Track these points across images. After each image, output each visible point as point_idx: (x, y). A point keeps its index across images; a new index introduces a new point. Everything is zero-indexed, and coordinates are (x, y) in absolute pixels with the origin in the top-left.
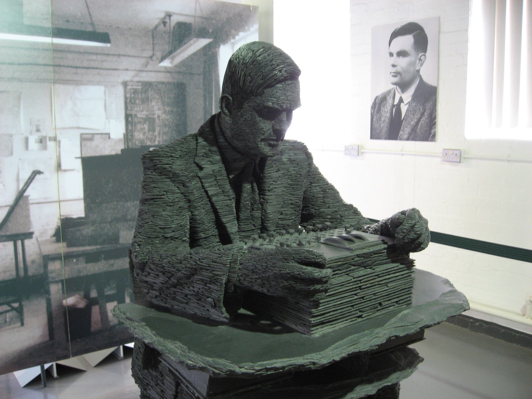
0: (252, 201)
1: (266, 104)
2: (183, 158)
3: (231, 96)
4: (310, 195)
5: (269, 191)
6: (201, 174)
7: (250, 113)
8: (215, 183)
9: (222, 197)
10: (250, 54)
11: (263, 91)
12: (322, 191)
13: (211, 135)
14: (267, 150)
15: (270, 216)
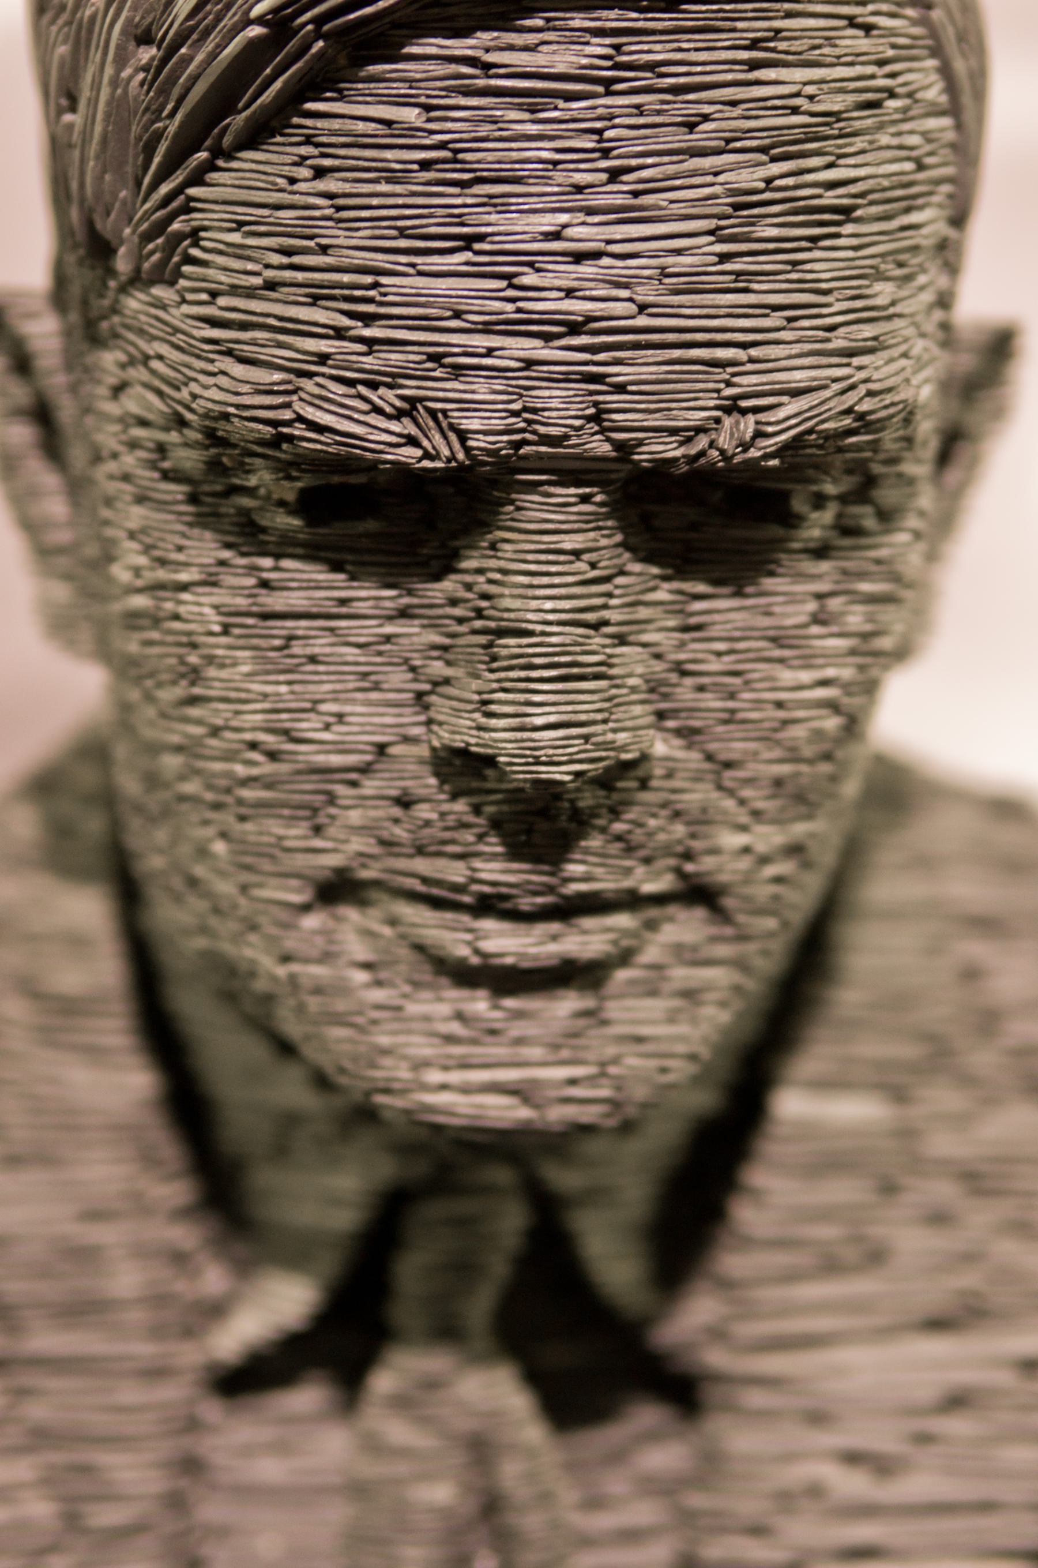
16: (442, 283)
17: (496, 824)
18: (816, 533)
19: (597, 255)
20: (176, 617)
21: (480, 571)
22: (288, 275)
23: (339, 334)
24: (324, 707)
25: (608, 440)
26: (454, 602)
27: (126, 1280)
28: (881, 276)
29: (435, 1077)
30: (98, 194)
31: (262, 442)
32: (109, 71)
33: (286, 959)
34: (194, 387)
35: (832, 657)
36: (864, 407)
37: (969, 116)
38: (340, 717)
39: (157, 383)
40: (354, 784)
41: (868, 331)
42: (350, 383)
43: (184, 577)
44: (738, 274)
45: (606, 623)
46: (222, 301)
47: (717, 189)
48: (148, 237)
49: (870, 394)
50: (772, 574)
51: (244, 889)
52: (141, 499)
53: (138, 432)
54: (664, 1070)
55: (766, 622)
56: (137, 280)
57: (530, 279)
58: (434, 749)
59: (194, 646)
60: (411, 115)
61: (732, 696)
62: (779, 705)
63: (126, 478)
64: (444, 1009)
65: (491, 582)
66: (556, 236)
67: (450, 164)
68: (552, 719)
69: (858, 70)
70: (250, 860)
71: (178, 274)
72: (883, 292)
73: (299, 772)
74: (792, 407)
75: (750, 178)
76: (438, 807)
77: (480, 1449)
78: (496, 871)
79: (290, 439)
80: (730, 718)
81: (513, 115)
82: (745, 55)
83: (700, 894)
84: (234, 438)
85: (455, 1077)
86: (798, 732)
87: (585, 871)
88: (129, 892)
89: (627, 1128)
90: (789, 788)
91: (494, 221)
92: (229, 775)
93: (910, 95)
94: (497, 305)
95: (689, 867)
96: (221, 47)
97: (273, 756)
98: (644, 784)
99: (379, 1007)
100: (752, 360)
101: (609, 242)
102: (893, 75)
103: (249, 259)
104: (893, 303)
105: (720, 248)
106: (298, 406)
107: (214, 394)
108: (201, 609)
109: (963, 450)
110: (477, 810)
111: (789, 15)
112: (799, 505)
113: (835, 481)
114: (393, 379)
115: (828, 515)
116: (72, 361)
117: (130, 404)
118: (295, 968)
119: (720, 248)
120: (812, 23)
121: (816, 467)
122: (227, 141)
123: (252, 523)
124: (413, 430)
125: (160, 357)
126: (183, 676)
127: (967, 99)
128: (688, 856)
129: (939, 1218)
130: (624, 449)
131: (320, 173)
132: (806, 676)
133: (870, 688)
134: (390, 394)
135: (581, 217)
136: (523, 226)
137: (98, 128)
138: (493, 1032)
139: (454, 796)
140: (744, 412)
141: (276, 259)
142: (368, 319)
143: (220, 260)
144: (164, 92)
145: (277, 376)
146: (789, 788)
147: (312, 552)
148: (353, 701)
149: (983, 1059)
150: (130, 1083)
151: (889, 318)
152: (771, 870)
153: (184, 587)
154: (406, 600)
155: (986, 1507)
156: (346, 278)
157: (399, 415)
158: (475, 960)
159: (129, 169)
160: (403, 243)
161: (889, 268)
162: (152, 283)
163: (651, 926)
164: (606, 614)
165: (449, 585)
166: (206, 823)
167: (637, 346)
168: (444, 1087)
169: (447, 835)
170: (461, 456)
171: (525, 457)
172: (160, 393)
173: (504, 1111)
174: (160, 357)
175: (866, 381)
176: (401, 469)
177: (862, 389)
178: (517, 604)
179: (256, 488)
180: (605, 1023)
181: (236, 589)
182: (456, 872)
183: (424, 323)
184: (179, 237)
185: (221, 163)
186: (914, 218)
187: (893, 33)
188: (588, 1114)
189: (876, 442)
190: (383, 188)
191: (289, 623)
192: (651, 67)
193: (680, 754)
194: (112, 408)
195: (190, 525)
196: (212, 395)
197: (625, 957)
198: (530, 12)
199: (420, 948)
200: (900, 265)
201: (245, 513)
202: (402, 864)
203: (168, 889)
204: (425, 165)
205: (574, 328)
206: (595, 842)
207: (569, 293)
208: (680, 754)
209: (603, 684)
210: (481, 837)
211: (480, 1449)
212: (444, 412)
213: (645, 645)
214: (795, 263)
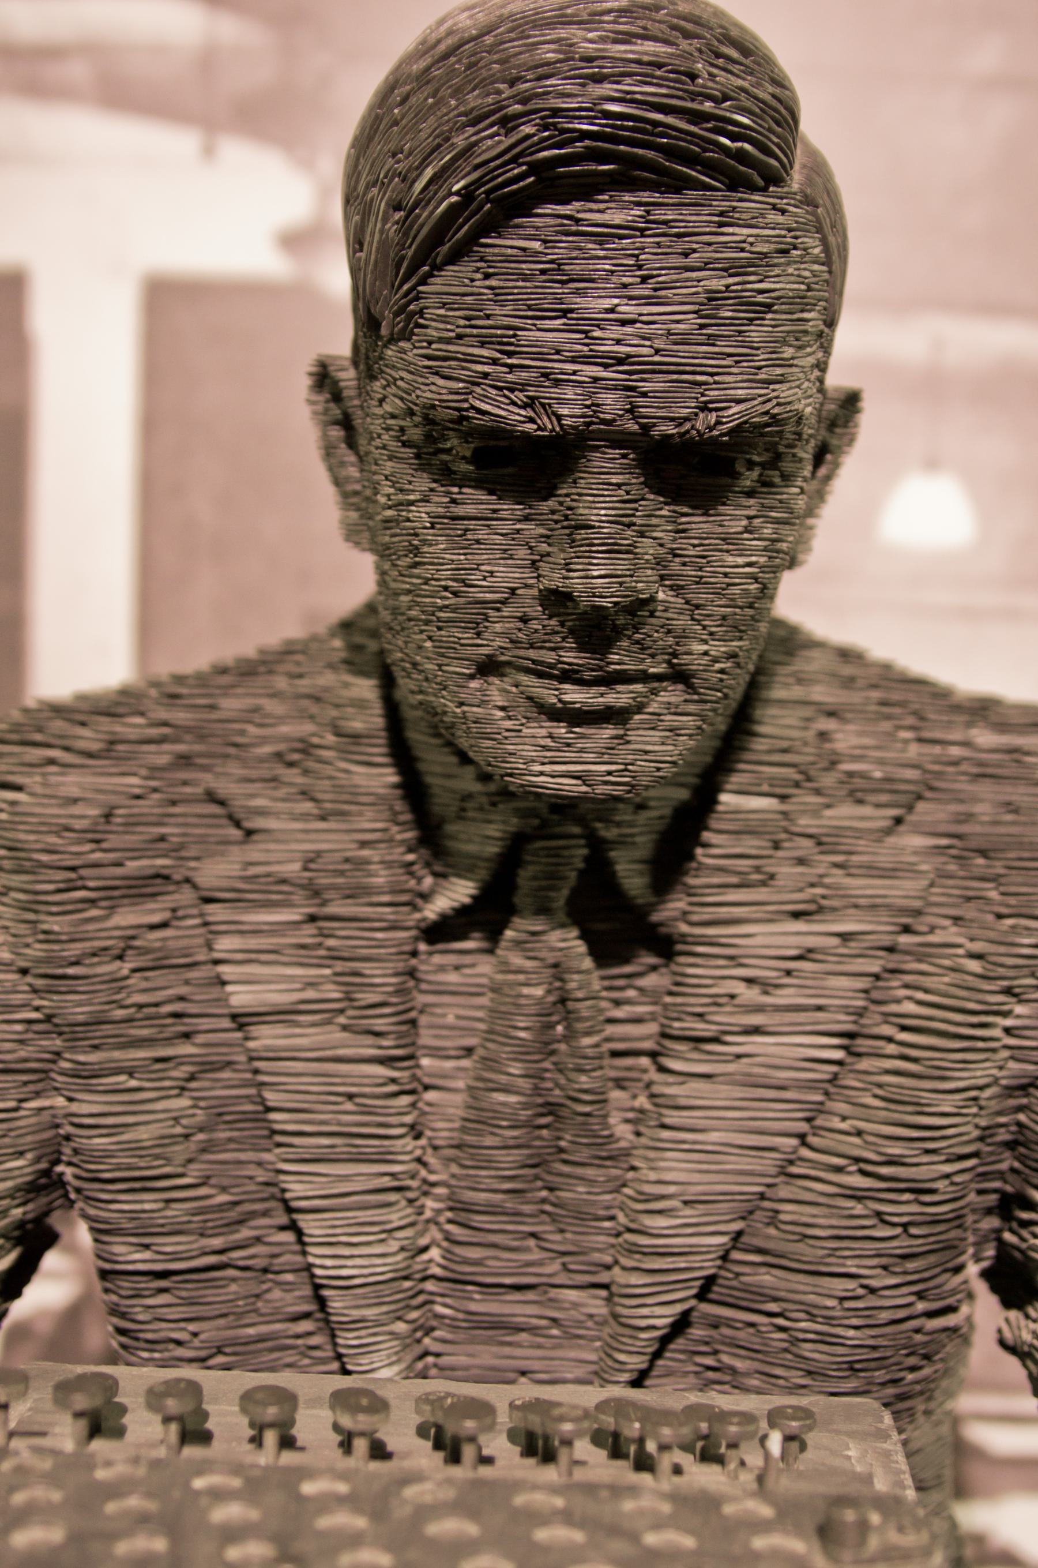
8: (307, 935)
9: (331, 1037)
16: (549, 335)
17: (572, 632)
18: (748, 483)
19: (633, 322)
20: (408, 520)
21: (567, 495)
22: (468, 330)
23: (495, 362)
24: (483, 568)
25: (637, 423)
27: (380, 880)
28: (785, 343)
29: (538, 768)
30: (372, 294)
31: (451, 421)
32: (379, 225)
33: (461, 704)
34: (418, 392)
35: (754, 550)
36: (776, 411)
37: (836, 267)
38: (492, 572)
39: (401, 393)
40: (498, 610)
41: (779, 371)
42: (500, 389)
43: (412, 497)
44: (709, 335)
45: (634, 524)
46: (434, 346)
47: (700, 289)
48: (397, 314)
49: (778, 404)
50: (724, 504)
51: (440, 666)
52: (391, 458)
53: (390, 422)
54: (658, 769)
55: (720, 530)
56: (392, 340)
57: (597, 333)
58: (540, 591)
59: (416, 535)
60: (536, 245)
61: (701, 569)
62: (726, 575)
63: (384, 447)
64: (543, 732)
65: (573, 500)
66: (612, 311)
67: (556, 272)
68: (603, 572)
69: (777, 232)
70: (444, 651)
71: (413, 334)
72: (788, 352)
73: (470, 603)
74: (736, 409)
75: (717, 284)
77: (558, 970)
78: (571, 657)
79: (467, 418)
81: (590, 246)
82: (716, 219)
83: (681, 676)
84: (438, 419)
85: (547, 768)
86: (736, 590)
87: (619, 659)
88: (387, 681)
89: (641, 807)
90: (730, 622)
91: (579, 302)
92: (434, 605)
93: (805, 250)
94: (579, 347)
95: (675, 661)
96: (437, 207)
97: (456, 594)
98: (652, 615)
99: (508, 730)
100: (715, 383)
101: (640, 315)
102: (796, 238)
103: (449, 323)
104: (793, 358)
105: (699, 321)
107: (429, 395)
108: (420, 514)
109: (829, 457)
110: (562, 624)
111: (741, 200)
112: (740, 467)
113: (759, 454)
114: (523, 387)
115: (755, 474)
116: (362, 391)
117: (387, 407)
118: (465, 708)
119: (699, 321)
120: (753, 205)
121: (750, 445)
122: (439, 260)
123: (449, 469)
124: (532, 414)
125: (402, 379)
126: (411, 552)
127: (835, 257)
128: (675, 655)
130: (646, 428)
131: (487, 276)
132: (740, 560)
133: (776, 571)
134: (521, 395)
135: (625, 301)
136: (595, 304)
137: (373, 257)
138: (568, 745)
139: (550, 617)
140: (711, 410)
141: (462, 322)
142: (510, 354)
143: (433, 324)
144: (406, 234)
145: (461, 385)
146: (730, 622)
148: (498, 565)
149: (828, 780)
151: (791, 366)
152: (718, 666)
153: (412, 503)
155: (819, 1008)
156: (499, 332)
157: (525, 406)
158: (559, 705)
159: (389, 279)
160: (530, 313)
161: (791, 339)
162: (400, 340)
163: (654, 692)
164: (634, 519)
165: (551, 503)
166: (422, 632)
167: (654, 372)
168: (542, 774)
169: (546, 637)
170: (558, 429)
171: (593, 431)
172: (402, 399)
173: (572, 787)
174: (402, 379)
175: (777, 397)
177: (775, 402)
178: (586, 511)
179: (450, 449)
180: (628, 742)
182: (550, 657)
183: (540, 356)
184: (413, 313)
186: (806, 315)
187: (796, 215)
188: (618, 791)
189: (782, 432)
190: (520, 284)
192: (665, 223)
193: (672, 599)
194: (379, 411)
195: (416, 470)
196: (427, 395)
197: (640, 708)
198: (602, 192)
199: (530, 698)
200: (797, 340)
201: (445, 463)
202: (522, 653)
203: (404, 669)
204: (543, 272)
205: (621, 361)
206: (625, 644)
207: (618, 342)
208: (672, 599)
209: (631, 556)
210: (564, 639)
211: (558, 970)
212: (549, 405)
213: (654, 538)
214: (740, 332)
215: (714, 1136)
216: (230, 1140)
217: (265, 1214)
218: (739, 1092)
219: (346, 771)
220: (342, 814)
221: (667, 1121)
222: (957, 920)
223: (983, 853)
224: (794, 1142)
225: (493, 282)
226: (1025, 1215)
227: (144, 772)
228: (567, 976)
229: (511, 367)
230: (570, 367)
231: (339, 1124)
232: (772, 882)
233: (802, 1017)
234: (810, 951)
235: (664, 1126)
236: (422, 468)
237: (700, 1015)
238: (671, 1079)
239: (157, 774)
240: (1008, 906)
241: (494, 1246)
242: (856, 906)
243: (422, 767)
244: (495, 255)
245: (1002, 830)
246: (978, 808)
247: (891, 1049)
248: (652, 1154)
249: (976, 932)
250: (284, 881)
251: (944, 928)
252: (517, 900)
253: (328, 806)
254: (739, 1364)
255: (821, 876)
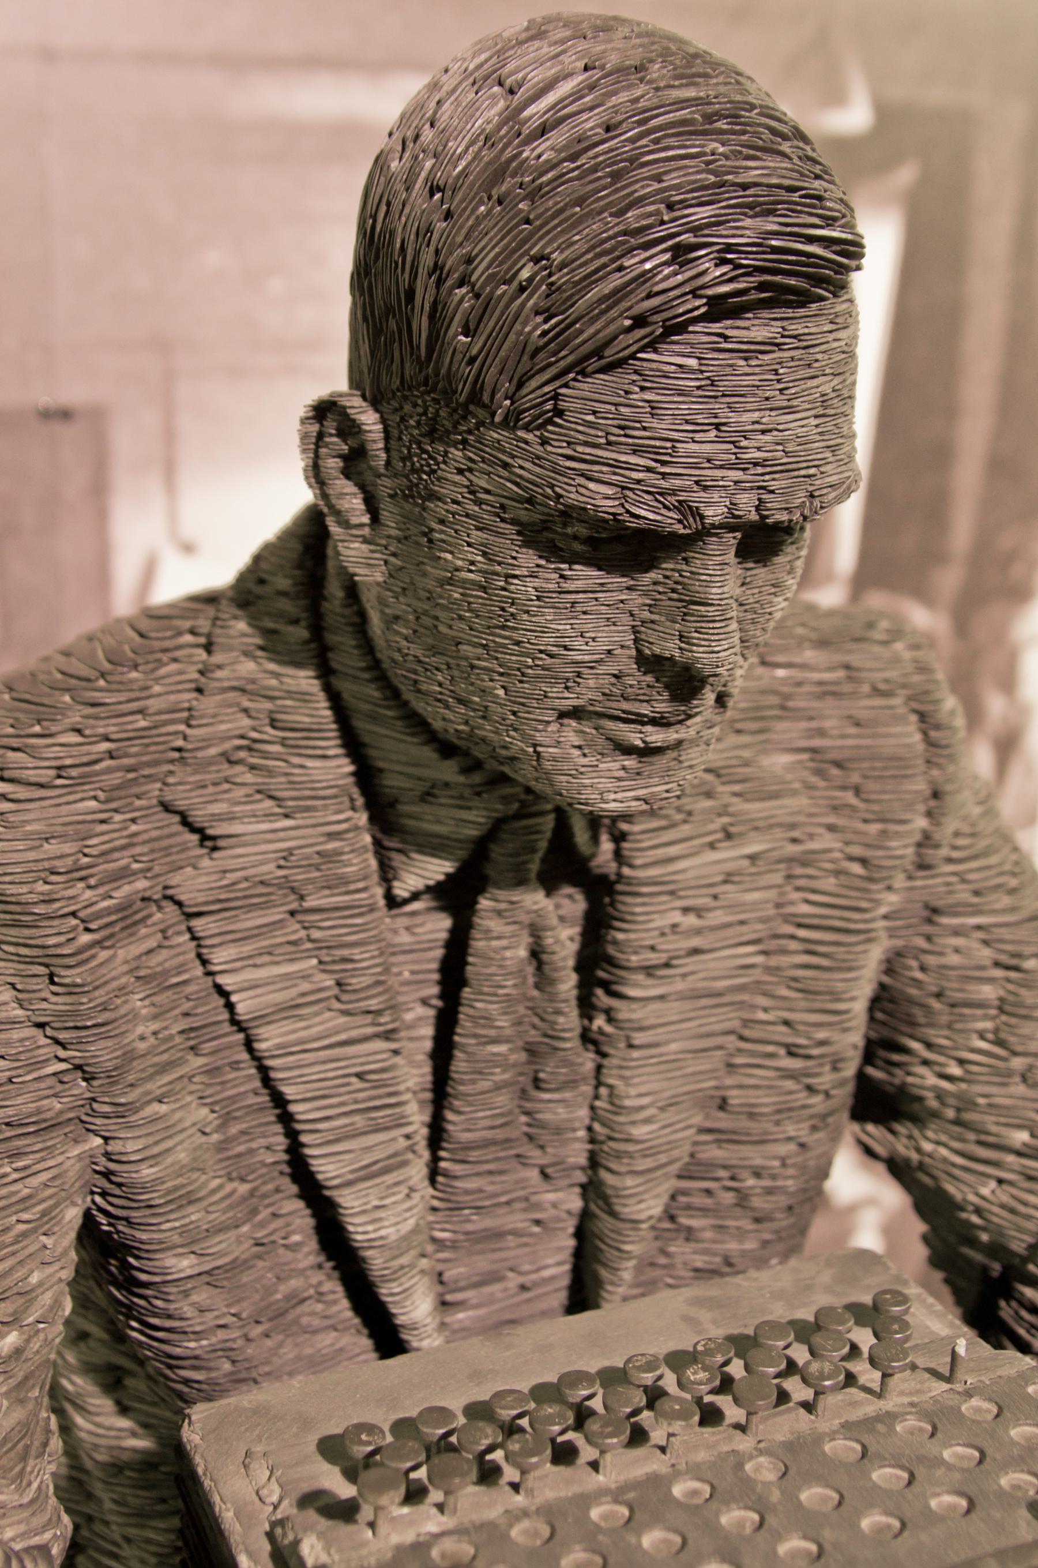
0: (534, 1036)
1: (573, 497)
2: (83, 780)
3: (375, 402)
4: (917, 983)
5: (649, 970)
6: (195, 882)
7: (476, 536)
8: (294, 930)
9: (329, 1022)
10: (491, 110)
11: (556, 397)
12: (997, 964)
13: (295, 622)
14: (605, 784)
15: (639, 1131)
17: (667, 687)
19: (770, 431)
22: (623, 439)
23: (649, 470)
26: (655, 583)
29: (612, 796)
38: (594, 639)
40: (592, 668)
60: (693, 362)
76: (637, 679)
80: (754, 622)
85: (619, 796)
96: (604, 327)
106: (627, 505)
114: (674, 492)
123: (556, 546)
129: (709, 795)
130: (763, 518)
131: (643, 389)
135: (768, 413)
139: (645, 673)
142: (664, 463)
147: (588, 562)
150: (337, 769)
154: (632, 583)
155: (742, 923)
156: (658, 443)
158: (642, 745)
165: (653, 575)
167: (782, 472)
176: (673, 535)
178: (700, 589)
181: (549, 580)
182: (645, 710)
185: (579, 378)
190: (676, 399)
191: (573, 596)
198: (748, 311)
201: (552, 541)
202: (614, 705)
204: (698, 388)
205: (755, 464)
215: (673, 1047)
216: (243, 1133)
217: (277, 1190)
218: (688, 1005)
219: (302, 767)
220: (308, 809)
221: (636, 1042)
222: (831, 828)
223: (838, 764)
224: (732, 1038)
225: (648, 396)
226: (896, 1057)
227: (101, 795)
228: (541, 933)
229: (664, 475)
230: (719, 473)
231: (356, 1102)
232: (691, 819)
233: (730, 932)
234: (729, 874)
235: (631, 1046)
236: (527, 544)
237: (653, 948)
238: (634, 1006)
239: (115, 794)
240: (873, 812)
241: (490, 1173)
242: (756, 829)
243: (372, 752)
244: (652, 370)
245: (849, 742)
246: (827, 724)
247: (793, 945)
248: (627, 1073)
249: (850, 836)
250: (262, 883)
251: (820, 835)
252: (490, 871)
253: (291, 803)
254: (694, 1223)
255: (726, 806)
